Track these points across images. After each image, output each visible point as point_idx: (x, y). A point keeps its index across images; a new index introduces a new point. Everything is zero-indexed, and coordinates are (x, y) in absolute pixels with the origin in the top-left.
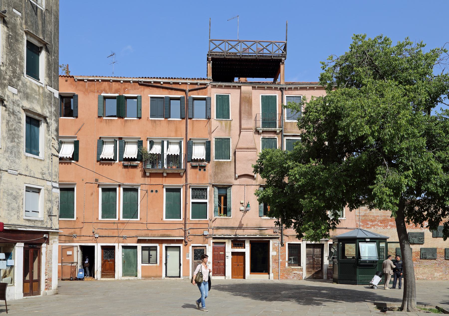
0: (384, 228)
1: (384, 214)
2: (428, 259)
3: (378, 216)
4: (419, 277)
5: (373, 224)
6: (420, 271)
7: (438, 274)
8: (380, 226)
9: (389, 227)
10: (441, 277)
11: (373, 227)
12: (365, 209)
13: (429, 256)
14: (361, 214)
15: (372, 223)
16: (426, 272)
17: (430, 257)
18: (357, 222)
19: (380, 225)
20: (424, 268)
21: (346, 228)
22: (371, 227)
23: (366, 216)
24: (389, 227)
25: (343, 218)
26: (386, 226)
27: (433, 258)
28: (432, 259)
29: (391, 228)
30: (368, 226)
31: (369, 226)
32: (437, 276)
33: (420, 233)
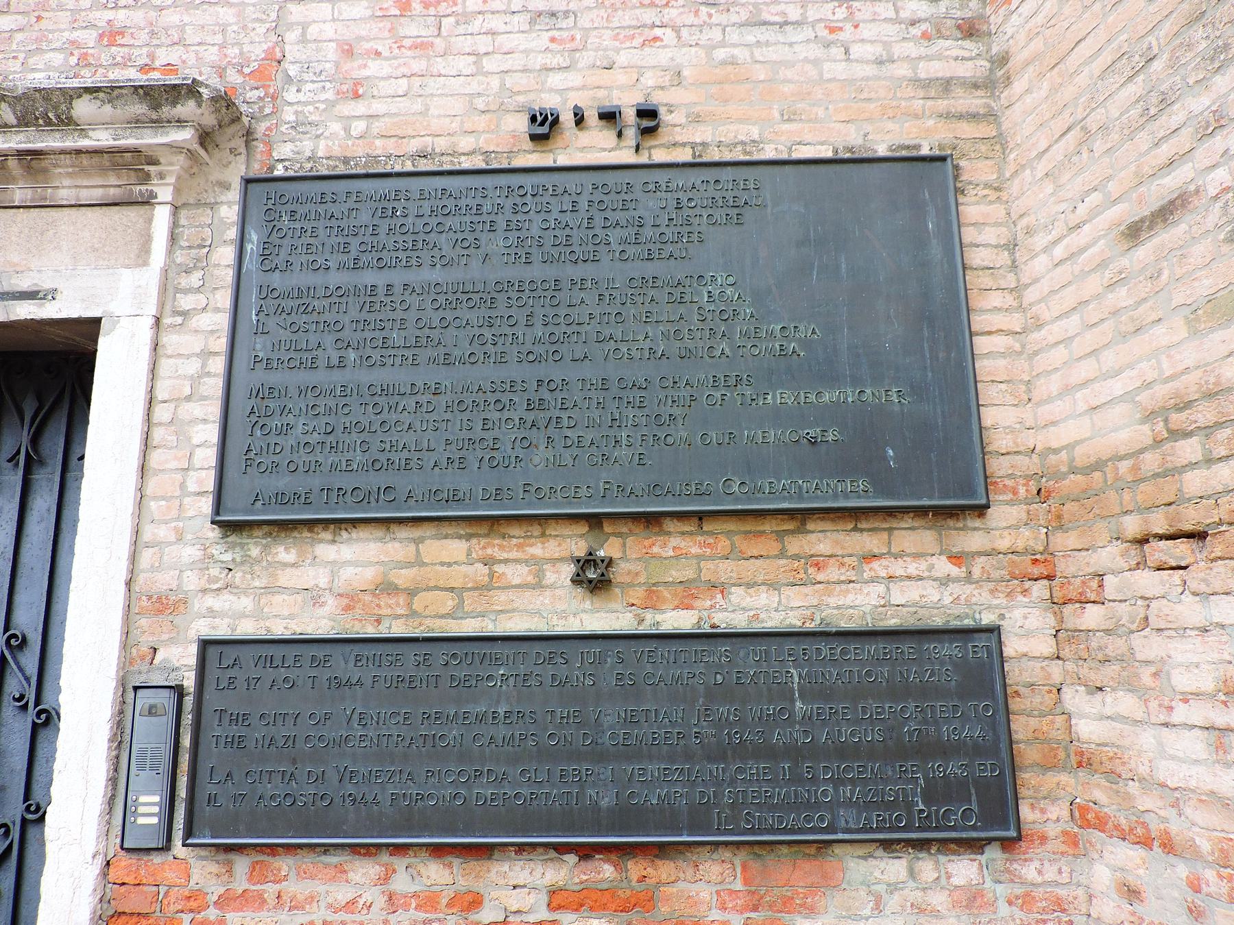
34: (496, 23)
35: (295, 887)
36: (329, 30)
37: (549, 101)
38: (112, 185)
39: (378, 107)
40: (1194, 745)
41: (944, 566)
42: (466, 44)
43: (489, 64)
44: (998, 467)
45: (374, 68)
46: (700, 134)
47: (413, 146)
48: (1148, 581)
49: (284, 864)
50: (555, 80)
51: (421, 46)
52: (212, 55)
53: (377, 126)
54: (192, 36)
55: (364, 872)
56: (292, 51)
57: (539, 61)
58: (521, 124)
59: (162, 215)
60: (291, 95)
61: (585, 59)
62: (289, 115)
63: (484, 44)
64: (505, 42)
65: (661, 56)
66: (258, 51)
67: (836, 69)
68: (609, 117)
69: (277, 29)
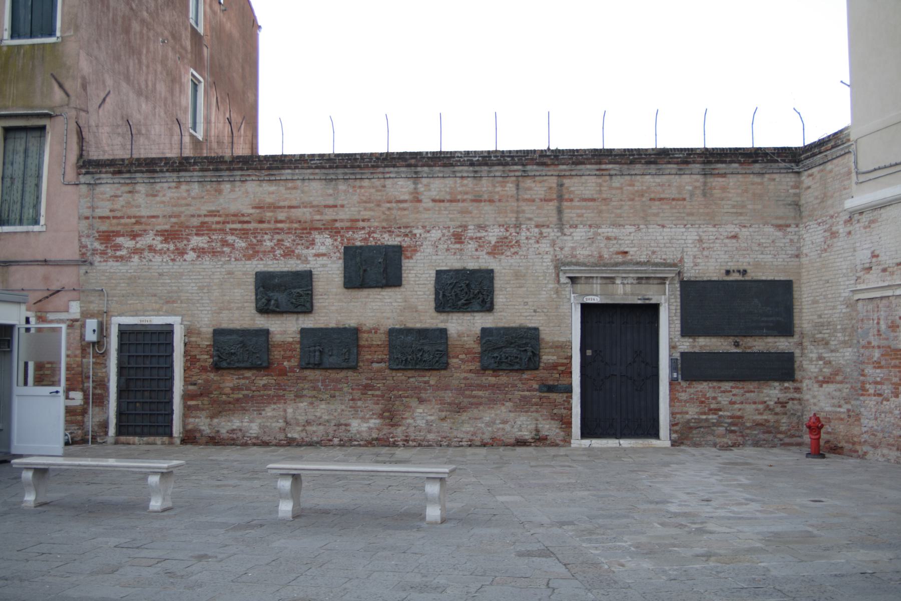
0: (173, 260)
1: (175, 209)
2: (326, 369)
3: (153, 217)
4: (296, 436)
5: (138, 246)
6: (300, 415)
7: (365, 425)
8: (161, 252)
9: (191, 256)
10: (375, 436)
11: (137, 257)
12: (112, 194)
13: (331, 359)
14: (99, 212)
15: (134, 242)
16: (320, 418)
17: (333, 360)
18: (83, 240)
19: (159, 247)
20: (312, 403)
21: (45, 261)
22: (130, 257)
23: (114, 218)
24: (191, 256)
25: (36, 228)
26: (182, 253)
27: (344, 365)
28: (342, 369)
29: (198, 257)
30: (118, 253)
31: (123, 252)
32: (359, 432)
33: (297, 275)
34: (719, 252)
35: (696, 386)
36: (691, 253)
37: (728, 268)
38: (659, 281)
39: (700, 268)
40: (813, 366)
41: (787, 344)
42: (714, 256)
43: (719, 260)
44: (796, 329)
45: (699, 261)
46: (753, 274)
47: (707, 275)
48: (812, 347)
49: (694, 383)
50: (729, 264)
51: (707, 257)
52: (671, 257)
53: (701, 271)
54: (668, 253)
55: (705, 384)
56: (685, 257)
57: (727, 260)
58: (724, 272)
59: (667, 286)
60: (686, 265)
61: (734, 260)
62: (685, 268)
63: (717, 257)
64: (721, 256)
65: (747, 260)
66: (679, 256)
67: (776, 263)
68: (739, 271)
69: (683, 252)
